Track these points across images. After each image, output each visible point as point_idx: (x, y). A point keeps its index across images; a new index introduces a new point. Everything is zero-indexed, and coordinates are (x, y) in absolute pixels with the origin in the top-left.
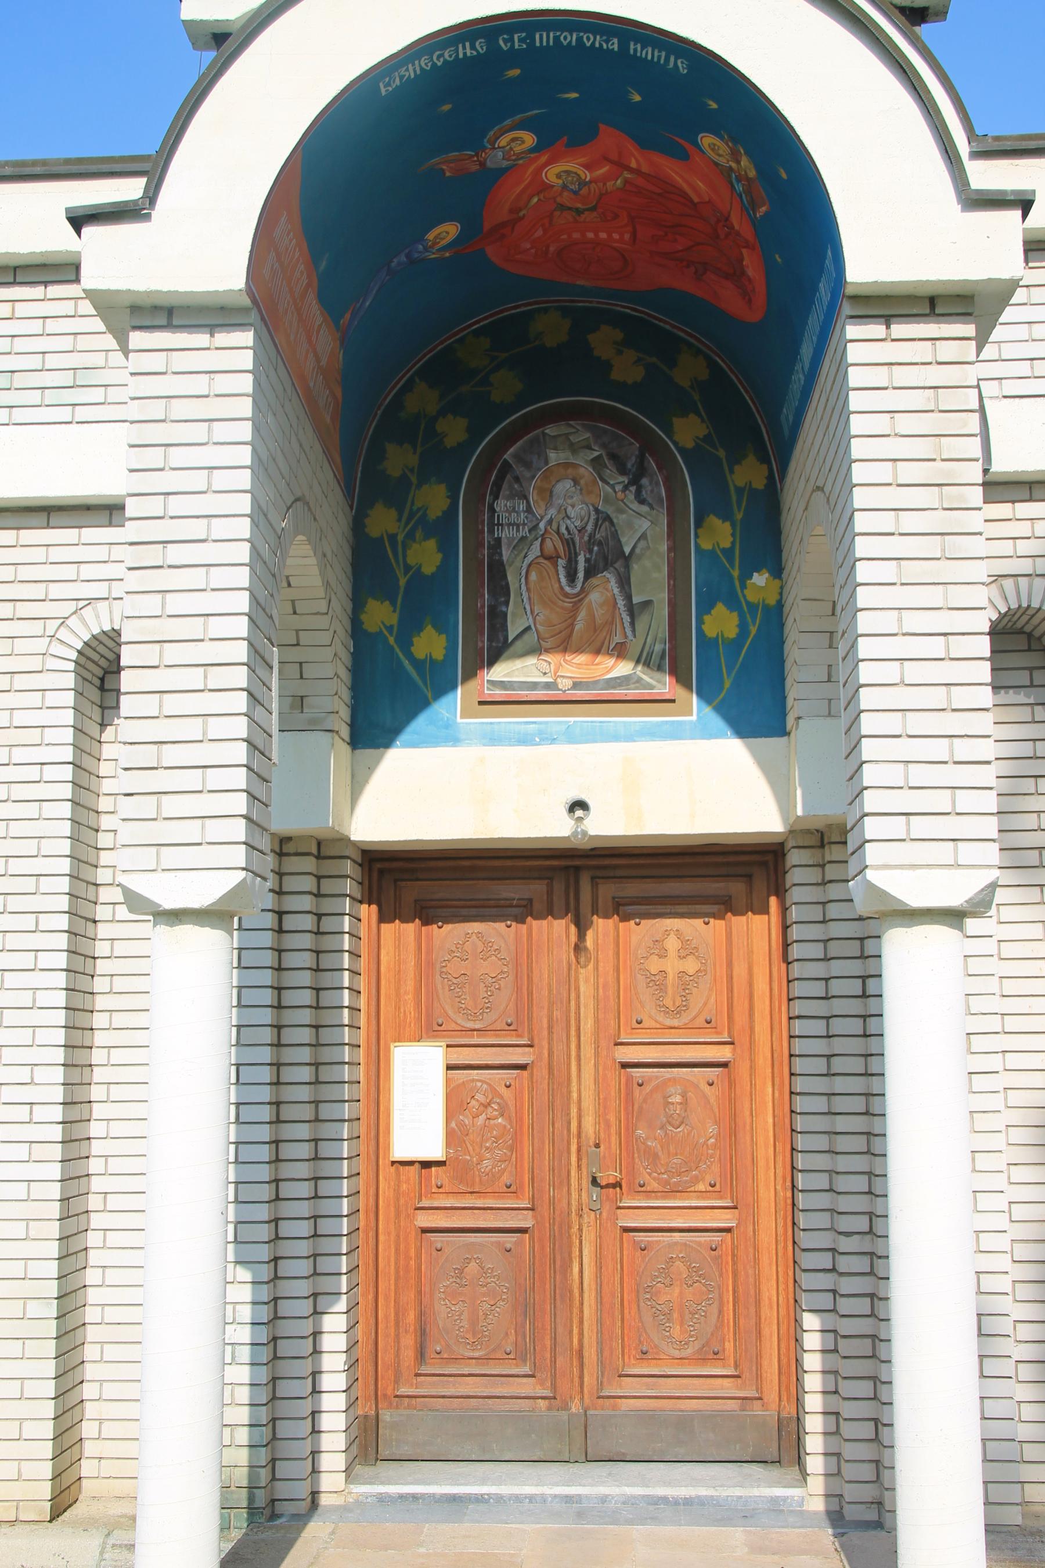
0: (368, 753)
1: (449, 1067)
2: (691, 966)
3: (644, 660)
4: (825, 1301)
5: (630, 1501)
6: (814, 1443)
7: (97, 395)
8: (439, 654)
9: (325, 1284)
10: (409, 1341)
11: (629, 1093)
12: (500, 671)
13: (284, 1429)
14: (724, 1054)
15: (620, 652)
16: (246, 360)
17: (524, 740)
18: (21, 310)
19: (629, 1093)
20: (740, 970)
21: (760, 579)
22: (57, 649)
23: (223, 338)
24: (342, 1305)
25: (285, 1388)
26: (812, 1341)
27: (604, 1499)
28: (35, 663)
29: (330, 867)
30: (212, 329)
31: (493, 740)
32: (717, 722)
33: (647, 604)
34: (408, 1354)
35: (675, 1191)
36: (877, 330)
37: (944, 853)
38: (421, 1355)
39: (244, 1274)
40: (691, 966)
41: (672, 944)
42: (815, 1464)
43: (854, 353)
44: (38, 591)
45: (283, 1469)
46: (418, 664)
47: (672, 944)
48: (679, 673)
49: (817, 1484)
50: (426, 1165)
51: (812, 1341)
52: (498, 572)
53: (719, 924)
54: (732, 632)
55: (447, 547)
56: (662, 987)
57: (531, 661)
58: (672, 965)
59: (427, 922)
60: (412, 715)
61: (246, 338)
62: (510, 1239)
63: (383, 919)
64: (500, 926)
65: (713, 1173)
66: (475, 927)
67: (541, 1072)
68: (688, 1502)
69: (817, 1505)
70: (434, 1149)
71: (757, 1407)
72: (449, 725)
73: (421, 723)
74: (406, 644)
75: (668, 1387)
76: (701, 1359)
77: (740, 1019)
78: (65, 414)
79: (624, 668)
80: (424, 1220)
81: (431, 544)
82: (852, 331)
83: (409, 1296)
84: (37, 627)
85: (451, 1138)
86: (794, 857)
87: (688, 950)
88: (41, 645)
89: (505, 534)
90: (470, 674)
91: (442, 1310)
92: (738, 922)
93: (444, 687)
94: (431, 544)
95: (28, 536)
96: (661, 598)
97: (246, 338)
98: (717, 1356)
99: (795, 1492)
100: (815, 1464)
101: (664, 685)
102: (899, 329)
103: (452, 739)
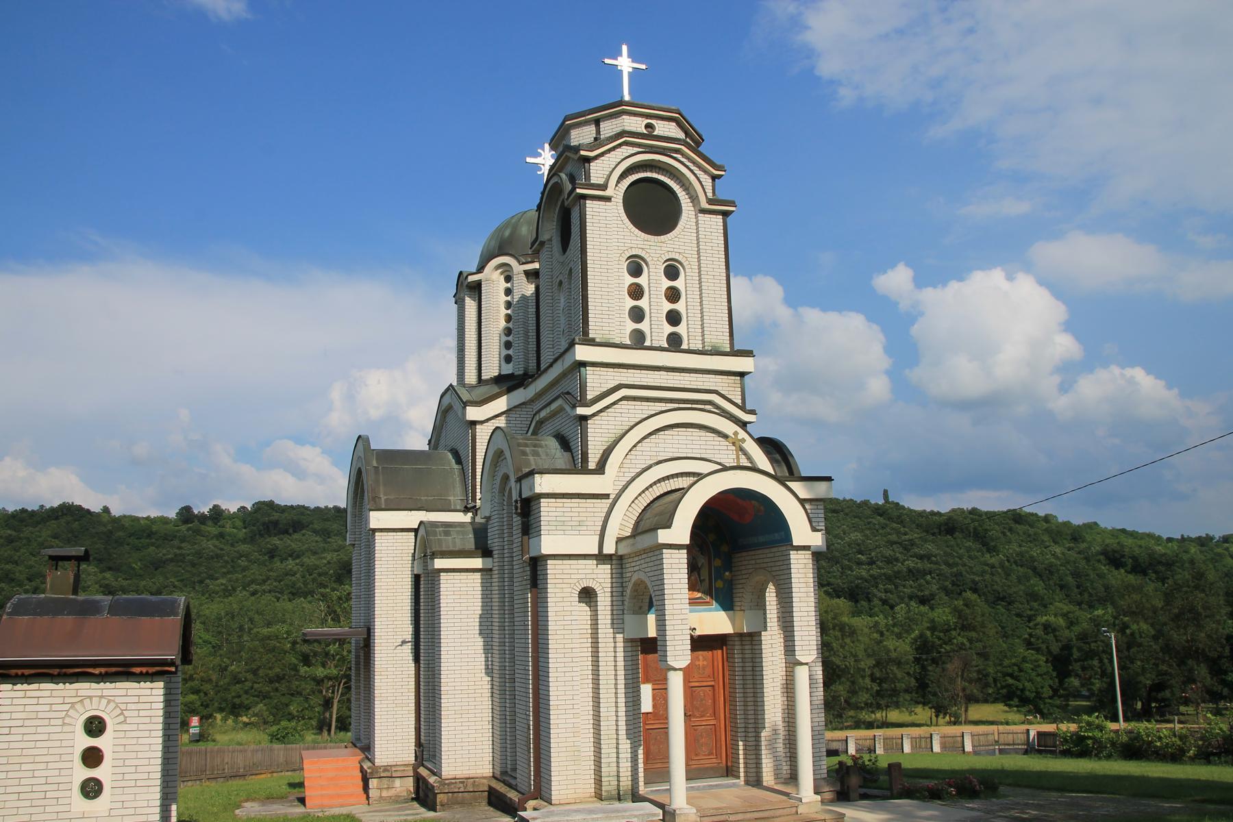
1: (653, 689)
2: (705, 663)
3: (703, 593)
4: (743, 739)
5: (704, 786)
7: (585, 528)
11: (692, 695)
14: (713, 683)
15: (698, 591)
16: (686, 556)
18: (566, 505)
19: (692, 695)
20: (716, 663)
21: (727, 573)
22: (574, 591)
23: (681, 551)
27: (699, 786)
28: (569, 595)
32: (719, 607)
33: (704, 580)
35: (702, 716)
36: (795, 552)
37: (808, 652)
39: (629, 741)
40: (705, 663)
41: (701, 658)
42: (742, 774)
44: (568, 576)
47: (701, 658)
48: (712, 597)
49: (742, 779)
50: (648, 713)
53: (710, 652)
54: (721, 586)
56: (699, 668)
58: (701, 663)
65: (711, 711)
68: (716, 785)
69: (743, 783)
70: (650, 710)
71: (721, 765)
75: (702, 762)
77: (716, 674)
78: (577, 533)
79: (699, 595)
80: (647, 727)
82: (791, 552)
84: (569, 586)
85: (654, 706)
87: (705, 659)
88: (570, 590)
92: (715, 652)
95: (565, 562)
96: (707, 581)
98: (712, 754)
99: (738, 781)
100: (742, 774)
101: (708, 599)
102: (799, 552)
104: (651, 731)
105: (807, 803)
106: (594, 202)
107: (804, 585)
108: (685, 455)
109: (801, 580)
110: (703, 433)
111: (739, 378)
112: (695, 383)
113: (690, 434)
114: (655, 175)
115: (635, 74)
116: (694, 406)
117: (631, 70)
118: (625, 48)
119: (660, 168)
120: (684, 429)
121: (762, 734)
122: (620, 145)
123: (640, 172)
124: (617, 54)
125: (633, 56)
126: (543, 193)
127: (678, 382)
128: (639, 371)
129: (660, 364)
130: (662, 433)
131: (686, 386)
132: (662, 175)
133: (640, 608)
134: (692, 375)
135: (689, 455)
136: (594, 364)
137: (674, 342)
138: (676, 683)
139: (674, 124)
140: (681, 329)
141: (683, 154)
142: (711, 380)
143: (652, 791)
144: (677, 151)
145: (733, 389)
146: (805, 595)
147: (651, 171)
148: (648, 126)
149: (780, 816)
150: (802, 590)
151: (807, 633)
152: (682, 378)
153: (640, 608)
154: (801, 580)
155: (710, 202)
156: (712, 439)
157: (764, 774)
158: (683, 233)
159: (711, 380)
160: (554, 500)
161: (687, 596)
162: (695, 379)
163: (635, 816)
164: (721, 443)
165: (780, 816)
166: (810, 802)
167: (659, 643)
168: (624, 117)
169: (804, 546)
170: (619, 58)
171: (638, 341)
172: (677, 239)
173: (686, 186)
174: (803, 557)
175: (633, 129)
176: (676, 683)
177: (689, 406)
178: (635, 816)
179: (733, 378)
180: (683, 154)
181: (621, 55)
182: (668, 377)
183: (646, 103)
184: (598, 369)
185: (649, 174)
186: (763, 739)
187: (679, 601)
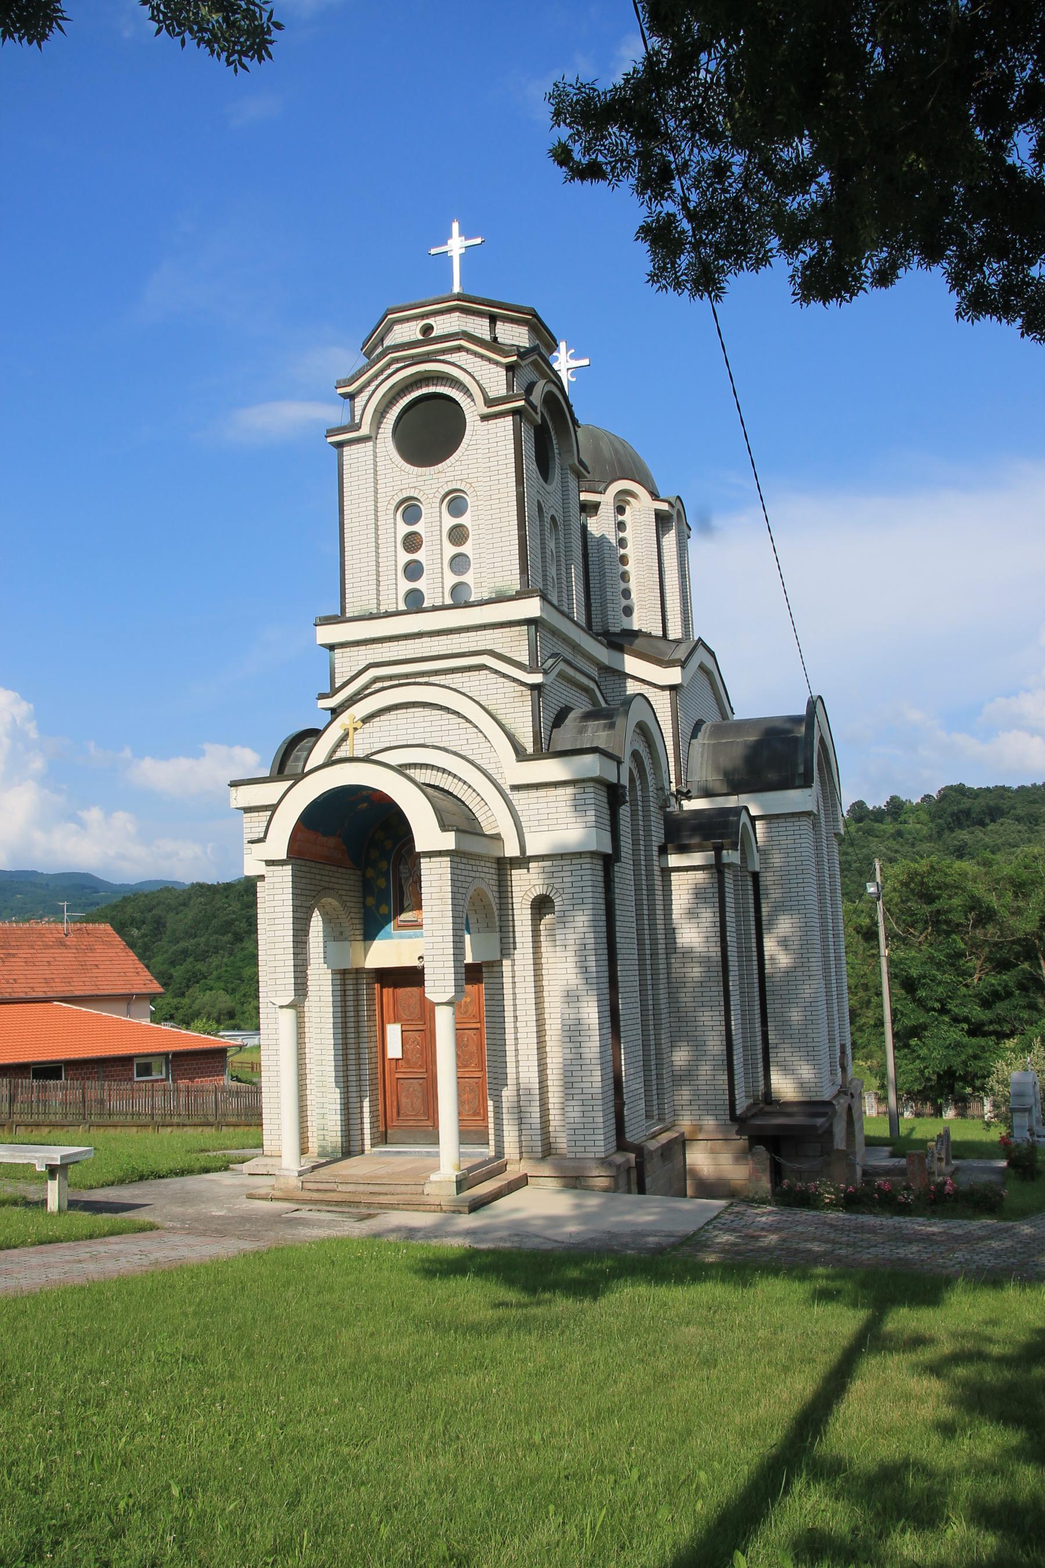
0: (368, 942)
6: (492, 1137)
8: (386, 912)
9: (363, 1094)
10: (395, 1110)
12: (404, 917)
13: (352, 1132)
14: (478, 1025)
16: (290, 873)
17: (410, 937)
23: (285, 867)
24: (368, 1099)
25: (351, 1122)
26: (491, 1109)
29: (360, 976)
30: (282, 865)
31: (401, 937)
34: (395, 1114)
35: (465, 1066)
36: (428, 860)
37: (442, 989)
38: (398, 1114)
42: (492, 1143)
43: (422, 866)
45: (352, 1143)
46: (381, 915)
50: (398, 1060)
51: (491, 1109)
52: (401, 887)
55: (388, 880)
57: (410, 913)
59: (395, 987)
60: (380, 931)
61: (290, 867)
62: (421, 1081)
63: (382, 987)
64: (415, 989)
65: (475, 1060)
66: (409, 989)
67: (428, 1032)
70: (400, 1056)
72: (390, 933)
73: (382, 933)
74: (378, 909)
76: (474, 1115)
81: (383, 879)
83: (394, 1098)
86: (484, 970)
89: (403, 876)
90: (394, 918)
91: (404, 1101)
93: (388, 922)
94: (383, 879)
97: (290, 867)
98: (478, 1114)
100: (492, 1143)
103: (389, 937)
104: (402, 1081)
105: (436, 1182)
106: (353, 447)
107: (439, 902)
108: (405, 743)
109: (434, 896)
110: (427, 712)
111: (526, 627)
112: (467, 645)
113: (412, 715)
114: (432, 389)
115: (469, 255)
116: (402, 681)
117: (463, 251)
118: (455, 226)
119: (438, 378)
120: (404, 711)
121: (504, 1093)
122: (388, 365)
123: (413, 391)
124: (444, 237)
125: (465, 233)
126: (569, 407)
127: (445, 647)
128: (396, 643)
129: (416, 630)
130: (378, 719)
131: (455, 651)
132: (442, 385)
133: (341, 933)
134: (462, 635)
135: (393, 744)
136: (343, 645)
137: (415, 603)
138: (444, 1021)
139: (457, 314)
140: (468, 578)
141: (467, 351)
142: (488, 637)
143: (381, 1152)
144: (459, 349)
145: (517, 643)
146: (439, 914)
147: (427, 385)
148: (427, 329)
149: (402, 1194)
150: (435, 908)
151: (441, 964)
152: (449, 642)
153: (341, 933)
154: (434, 896)
155: (489, 402)
156: (439, 717)
157: (506, 1145)
158: (467, 453)
159: (488, 637)
160: (256, 814)
161: (424, 915)
162: (483, 638)
163: (36, 1158)
164: (451, 722)
165: (402, 1194)
166: (440, 1182)
167: (463, 976)
168: (396, 327)
169: (440, 852)
170: (449, 242)
171: (415, 603)
172: (459, 463)
173: (467, 392)
174: (438, 865)
175: (406, 339)
176: (444, 1021)
177: (397, 682)
178: (36, 1158)
179: (518, 628)
180: (467, 351)
181: (449, 236)
182: (432, 644)
183: (412, 302)
184: (348, 649)
185: (424, 391)
186: (504, 1099)
187: (281, 927)
